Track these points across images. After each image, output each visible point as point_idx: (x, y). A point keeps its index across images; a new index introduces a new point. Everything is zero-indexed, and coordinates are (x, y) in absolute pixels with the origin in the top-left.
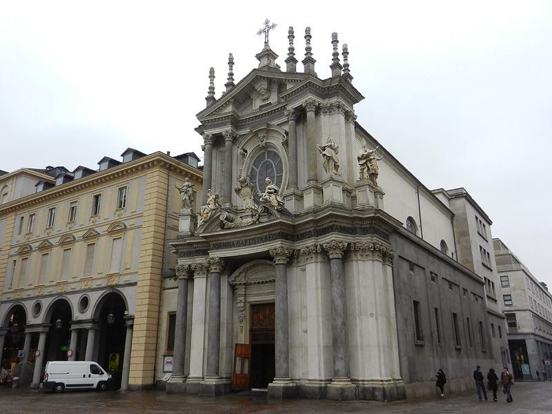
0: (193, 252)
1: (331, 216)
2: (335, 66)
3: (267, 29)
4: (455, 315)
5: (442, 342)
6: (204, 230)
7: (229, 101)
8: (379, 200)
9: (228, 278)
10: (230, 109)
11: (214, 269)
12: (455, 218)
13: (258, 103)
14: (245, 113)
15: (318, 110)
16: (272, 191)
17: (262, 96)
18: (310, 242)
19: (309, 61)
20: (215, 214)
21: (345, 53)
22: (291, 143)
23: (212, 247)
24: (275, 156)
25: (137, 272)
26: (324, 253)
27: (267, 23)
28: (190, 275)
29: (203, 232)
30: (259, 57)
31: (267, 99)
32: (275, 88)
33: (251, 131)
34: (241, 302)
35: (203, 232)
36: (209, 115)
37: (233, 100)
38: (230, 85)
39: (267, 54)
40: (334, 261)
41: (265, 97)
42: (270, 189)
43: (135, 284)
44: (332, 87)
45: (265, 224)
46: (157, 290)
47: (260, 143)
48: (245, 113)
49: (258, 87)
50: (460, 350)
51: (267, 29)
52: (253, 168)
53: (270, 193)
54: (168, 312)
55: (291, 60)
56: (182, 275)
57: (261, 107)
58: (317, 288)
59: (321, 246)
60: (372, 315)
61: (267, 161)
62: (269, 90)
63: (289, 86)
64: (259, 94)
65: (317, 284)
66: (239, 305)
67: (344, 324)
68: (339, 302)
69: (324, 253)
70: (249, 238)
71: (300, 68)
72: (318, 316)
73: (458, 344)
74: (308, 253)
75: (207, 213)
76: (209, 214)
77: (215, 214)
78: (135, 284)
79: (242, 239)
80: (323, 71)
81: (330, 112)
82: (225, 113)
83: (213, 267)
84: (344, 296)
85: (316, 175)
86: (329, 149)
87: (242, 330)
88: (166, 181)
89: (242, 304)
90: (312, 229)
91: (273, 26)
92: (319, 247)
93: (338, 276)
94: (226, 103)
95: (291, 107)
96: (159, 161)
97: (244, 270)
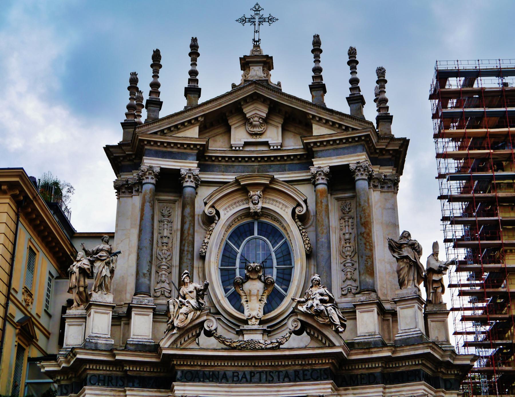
0: (117, 377)
1: (427, 356)
6: (175, 342)
7: (196, 119)
10: (193, 132)
13: (239, 136)
14: (217, 146)
16: (327, 298)
17: (255, 126)
24: (273, 233)
27: (257, 9)
31: (261, 134)
33: (237, 181)
36: (156, 133)
37: (203, 119)
38: (192, 91)
41: (256, 130)
42: (322, 295)
45: (287, 353)
47: (251, 205)
48: (217, 146)
49: (249, 111)
57: (247, 144)
61: (256, 238)
62: (266, 121)
63: (318, 130)
64: (246, 121)
70: (260, 369)
75: (187, 314)
76: (190, 316)
79: (246, 369)
81: (382, 187)
82: (186, 138)
86: (410, 250)
88: (13, 226)
90: (379, 370)
91: (271, 20)
94: (189, 122)
95: (323, 163)
96: (12, 186)
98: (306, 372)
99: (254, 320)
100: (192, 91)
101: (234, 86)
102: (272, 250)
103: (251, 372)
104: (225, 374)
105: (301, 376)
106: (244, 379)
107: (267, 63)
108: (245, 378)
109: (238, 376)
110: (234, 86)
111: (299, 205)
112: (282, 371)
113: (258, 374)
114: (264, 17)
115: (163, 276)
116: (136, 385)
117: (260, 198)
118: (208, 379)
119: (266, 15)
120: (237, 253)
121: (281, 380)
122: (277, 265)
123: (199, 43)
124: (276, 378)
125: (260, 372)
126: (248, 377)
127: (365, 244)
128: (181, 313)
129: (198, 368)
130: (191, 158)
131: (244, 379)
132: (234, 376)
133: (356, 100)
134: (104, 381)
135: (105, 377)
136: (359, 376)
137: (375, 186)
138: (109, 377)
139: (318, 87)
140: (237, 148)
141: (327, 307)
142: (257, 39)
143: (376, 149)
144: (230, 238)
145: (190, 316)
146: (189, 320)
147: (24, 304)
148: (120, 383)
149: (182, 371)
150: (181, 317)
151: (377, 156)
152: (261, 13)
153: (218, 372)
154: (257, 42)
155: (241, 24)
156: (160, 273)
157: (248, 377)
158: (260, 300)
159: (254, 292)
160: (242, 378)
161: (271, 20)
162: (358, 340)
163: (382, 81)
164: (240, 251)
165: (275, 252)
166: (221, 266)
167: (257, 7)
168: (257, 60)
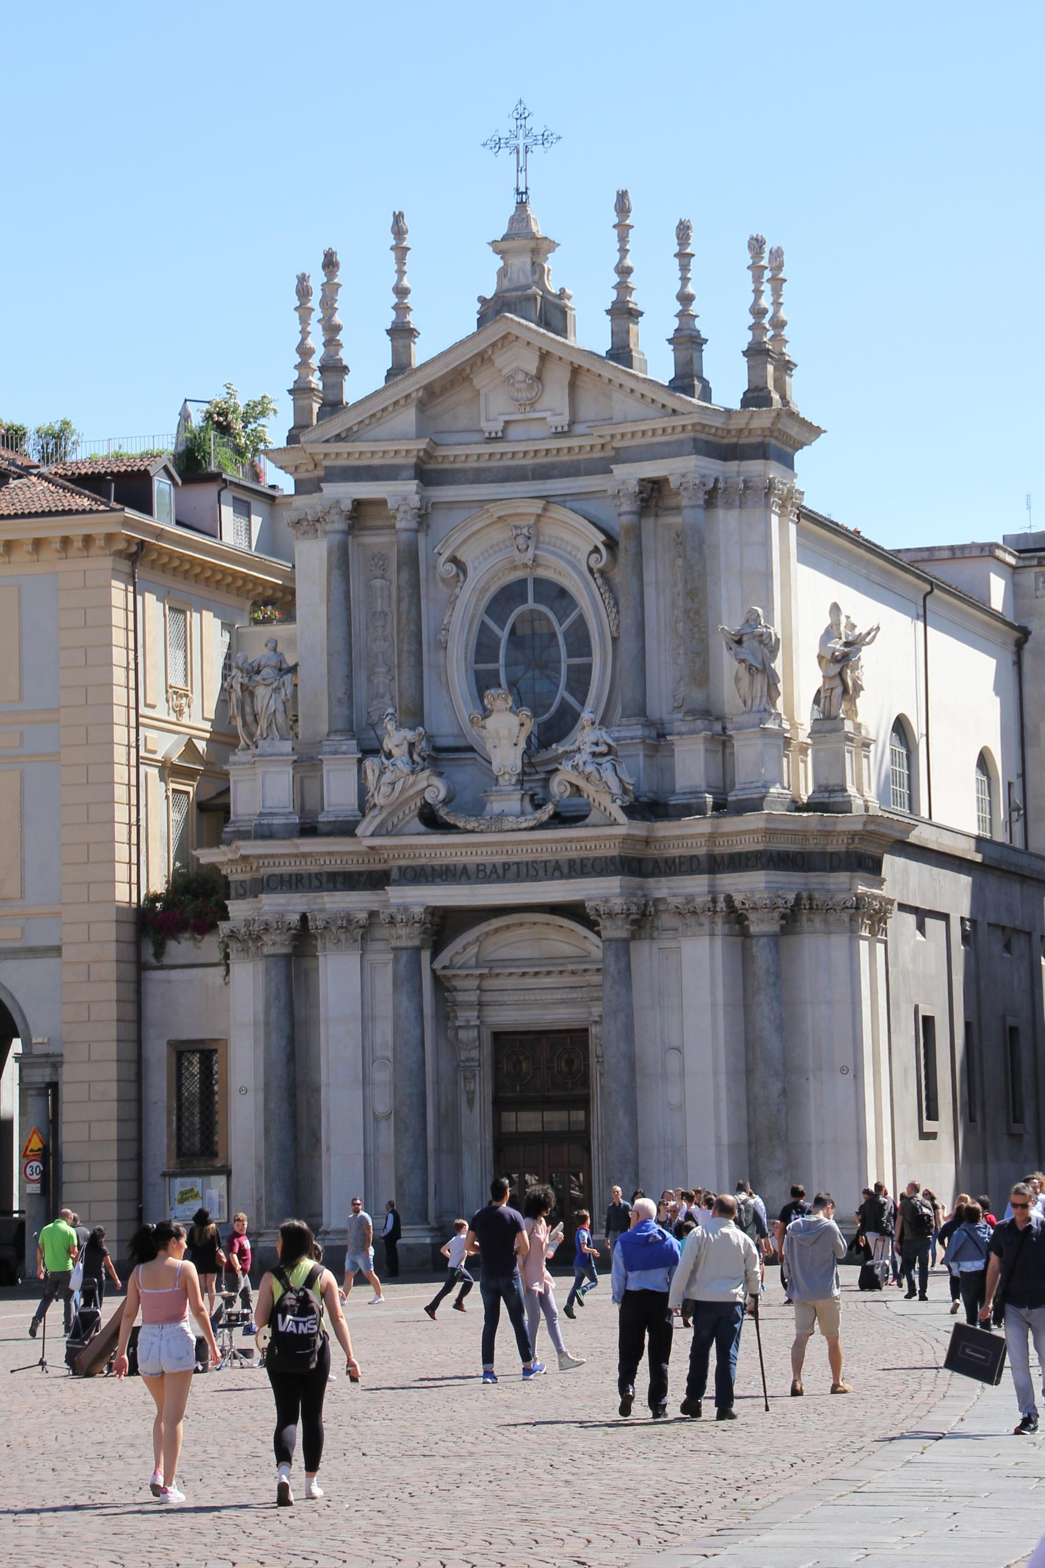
2: (756, 353)
3: (521, 141)
4: (1013, 1031)
5: (978, 1118)
8: (865, 760)
9: (432, 960)
11: (407, 937)
12: (1028, 646)
15: (712, 497)
16: (603, 749)
17: (519, 390)
18: (696, 885)
19: (688, 342)
20: (413, 785)
21: (777, 283)
22: (618, 576)
23: (395, 875)
25: (59, 914)
26: (736, 918)
28: (303, 938)
29: (372, 835)
30: (499, 248)
32: (558, 378)
34: (467, 1027)
35: (372, 835)
36: (338, 438)
38: (401, 333)
39: (522, 243)
40: (763, 941)
41: (524, 395)
43: (56, 950)
44: (750, 430)
46: (130, 971)
50: (1020, 1136)
51: (521, 141)
52: (483, 621)
53: (594, 754)
54: (169, 1042)
55: (623, 313)
56: (276, 944)
58: (714, 1004)
59: (729, 899)
60: (844, 1070)
65: (713, 994)
66: (463, 1035)
67: (784, 1092)
68: (773, 1042)
69: (736, 918)
71: (658, 363)
72: (715, 1073)
73: (1015, 1121)
74: (688, 911)
75: (393, 784)
77: (413, 785)
78: (56, 950)
80: (727, 381)
83: (403, 932)
84: (786, 1026)
85: (708, 698)
87: (471, 1103)
89: (473, 1034)
92: (721, 905)
93: (772, 979)
94: (396, 403)
95: (629, 475)
97: (478, 938)
98: (585, 862)
99: (507, 777)
100: (401, 333)
101: (482, 300)
102: (559, 630)
103: (504, 864)
104: (465, 867)
105: (578, 867)
106: (494, 875)
107: (539, 249)
108: (496, 872)
109: (484, 870)
110: (482, 300)
111: (596, 550)
112: (550, 861)
113: (515, 866)
114: (535, 132)
115: (381, 686)
116: (339, 886)
117: (529, 538)
118: (441, 877)
119: (538, 131)
120: (498, 641)
121: (549, 875)
122: (569, 656)
123: (408, 222)
124: (541, 872)
125: (518, 863)
126: (500, 871)
127: (691, 630)
128: (384, 784)
129: (423, 861)
130: (404, 474)
131: (494, 875)
132: (478, 871)
133: (688, 342)
134: (290, 881)
135: (290, 875)
136: (677, 860)
137: (729, 506)
138: (297, 875)
139: (623, 313)
140: (493, 435)
141: (600, 764)
142: (522, 189)
143: (729, 431)
144: (489, 611)
145: (399, 786)
146: (396, 793)
147: (173, 718)
148: (316, 883)
149: (400, 868)
150: (385, 789)
151: (734, 440)
152: (529, 123)
153: (455, 866)
154: (522, 193)
155: (491, 153)
156: (375, 681)
157: (500, 871)
158: (515, 745)
159: (503, 732)
160: (491, 872)
161: (545, 139)
162: (674, 801)
163: (765, 264)
164: (504, 635)
165: (566, 635)
166: (476, 662)
167: (521, 111)
168: (522, 243)
